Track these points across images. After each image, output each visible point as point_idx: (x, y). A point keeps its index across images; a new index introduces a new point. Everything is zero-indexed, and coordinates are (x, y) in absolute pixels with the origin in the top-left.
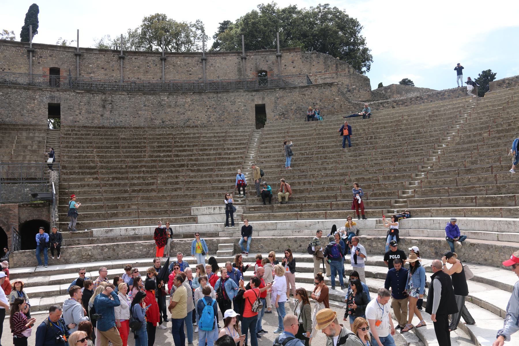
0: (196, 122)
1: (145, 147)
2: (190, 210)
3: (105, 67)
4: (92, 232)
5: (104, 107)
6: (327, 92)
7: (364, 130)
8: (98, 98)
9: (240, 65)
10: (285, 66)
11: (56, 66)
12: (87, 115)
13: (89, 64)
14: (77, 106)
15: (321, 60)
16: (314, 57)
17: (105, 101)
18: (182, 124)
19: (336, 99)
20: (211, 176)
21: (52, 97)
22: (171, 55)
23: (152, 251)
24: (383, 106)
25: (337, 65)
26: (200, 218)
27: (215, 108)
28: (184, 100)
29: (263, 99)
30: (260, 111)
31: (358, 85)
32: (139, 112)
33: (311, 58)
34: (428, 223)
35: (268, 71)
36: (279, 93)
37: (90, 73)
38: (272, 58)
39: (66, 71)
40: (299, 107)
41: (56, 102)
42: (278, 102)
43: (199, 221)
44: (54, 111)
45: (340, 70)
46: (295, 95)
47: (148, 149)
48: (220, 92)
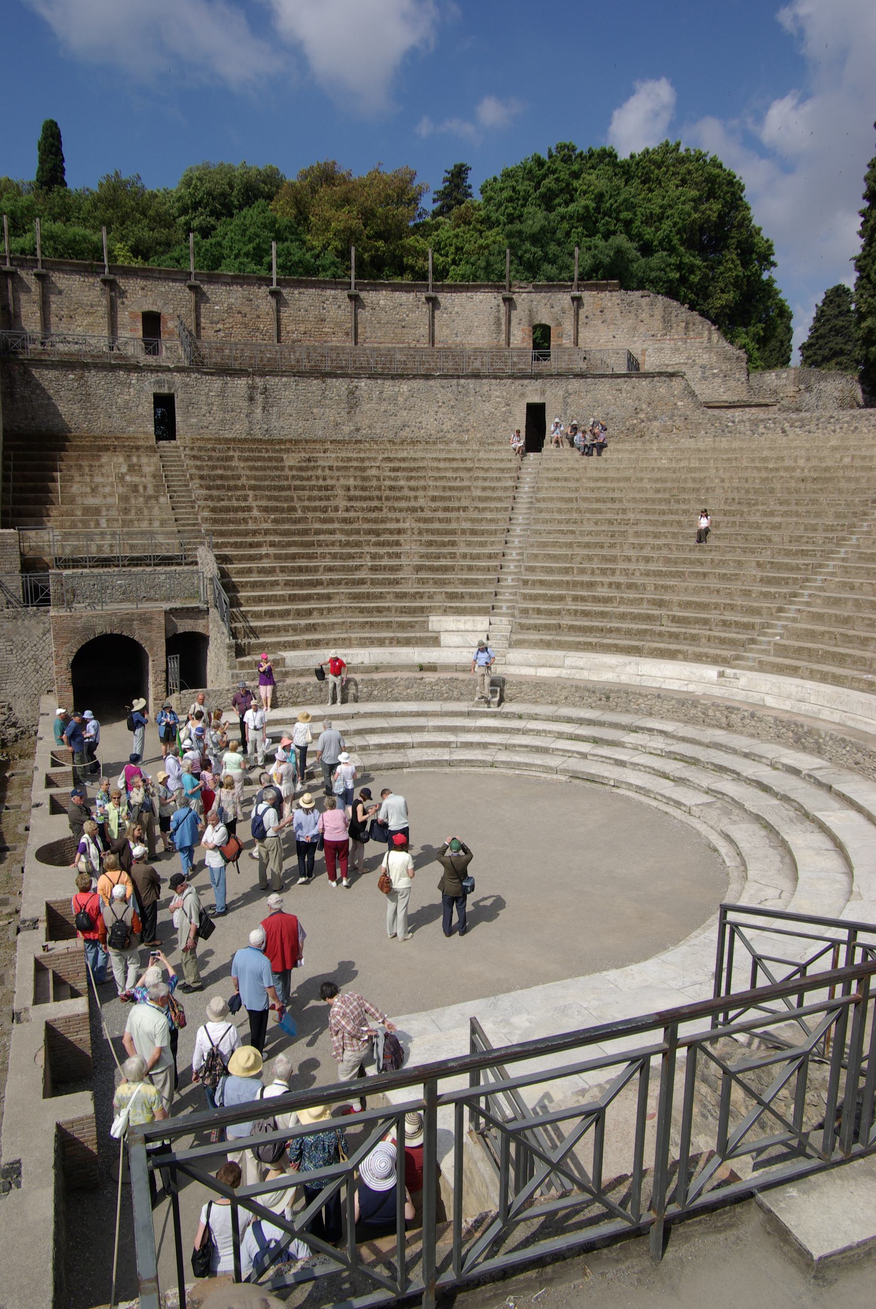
0: (416, 430)
1: (332, 488)
2: (427, 622)
3: (246, 310)
4: (283, 659)
5: (251, 399)
6: (662, 388)
7: (723, 481)
8: (242, 383)
9: (499, 311)
11: (154, 309)
12: (220, 416)
13: (216, 304)
14: (203, 398)
15: (658, 312)
16: (644, 304)
17: (253, 388)
18: (391, 435)
19: (679, 403)
20: (453, 556)
21: (158, 383)
23: (375, 693)
24: (765, 427)
25: (687, 324)
26: (445, 639)
27: (452, 407)
28: (396, 389)
29: (543, 393)
30: (536, 415)
31: (723, 367)
32: (315, 410)
33: (639, 305)
34: (794, 690)
35: (552, 325)
36: (575, 384)
38: (564, 299)
39: (172, 319)
41: (166, 391)
42: (569, 400)
43: (442, 643)
44: (164, 406)
45: (692, 334)
46: (603, 390)
47: (341, 492)
48: (463, 377)
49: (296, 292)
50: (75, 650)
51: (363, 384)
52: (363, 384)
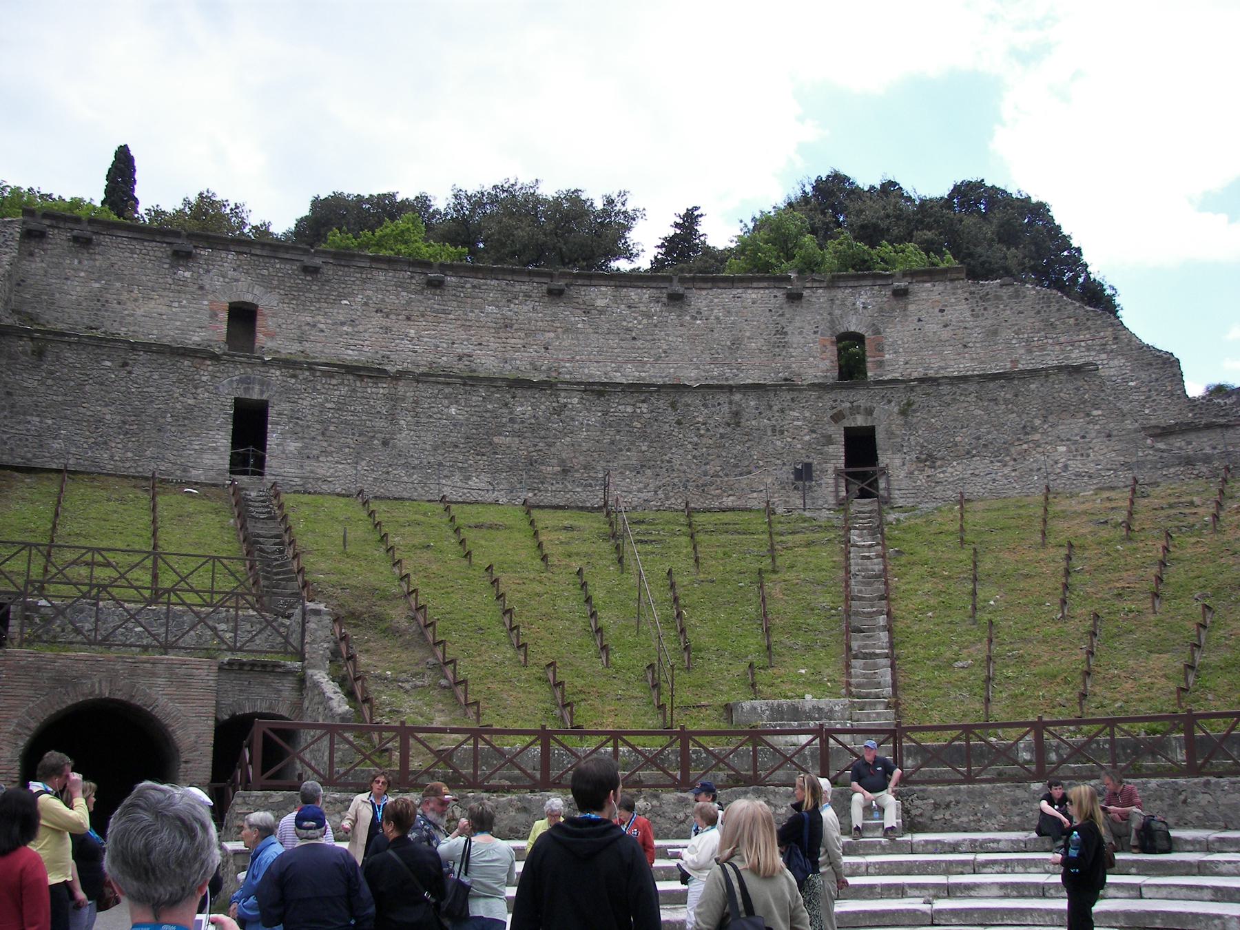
10: (920, 320)
11: (248, 298)
21: (246, 381)
22: (580, 282)
32: (496, 440)
35: (868, 335)
37: (343, 324)
40: (978, 438)
41: (255, 396)
49: (468, 285)
50: (34, 725)
51: (575, 400)
52: (575, 400)
